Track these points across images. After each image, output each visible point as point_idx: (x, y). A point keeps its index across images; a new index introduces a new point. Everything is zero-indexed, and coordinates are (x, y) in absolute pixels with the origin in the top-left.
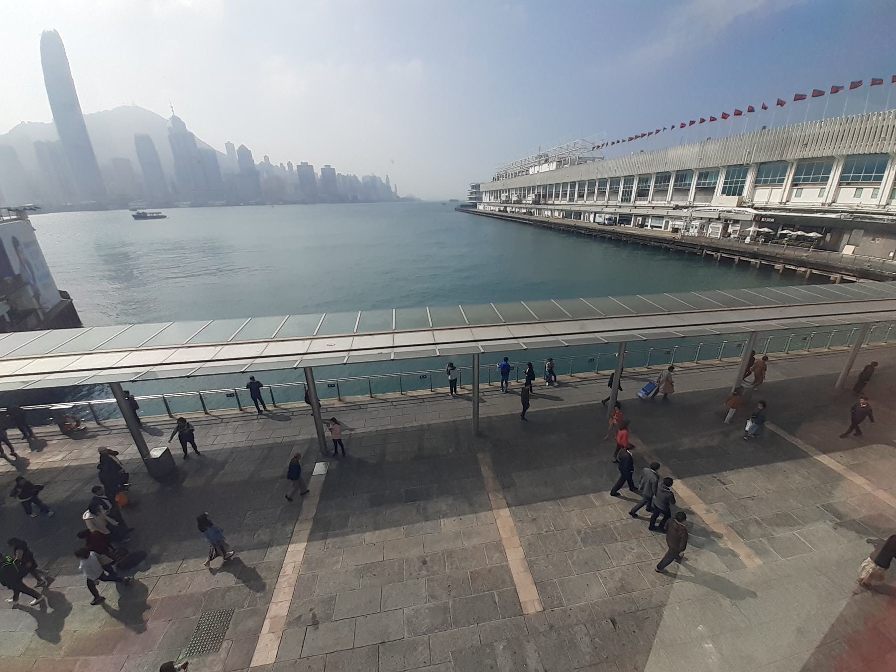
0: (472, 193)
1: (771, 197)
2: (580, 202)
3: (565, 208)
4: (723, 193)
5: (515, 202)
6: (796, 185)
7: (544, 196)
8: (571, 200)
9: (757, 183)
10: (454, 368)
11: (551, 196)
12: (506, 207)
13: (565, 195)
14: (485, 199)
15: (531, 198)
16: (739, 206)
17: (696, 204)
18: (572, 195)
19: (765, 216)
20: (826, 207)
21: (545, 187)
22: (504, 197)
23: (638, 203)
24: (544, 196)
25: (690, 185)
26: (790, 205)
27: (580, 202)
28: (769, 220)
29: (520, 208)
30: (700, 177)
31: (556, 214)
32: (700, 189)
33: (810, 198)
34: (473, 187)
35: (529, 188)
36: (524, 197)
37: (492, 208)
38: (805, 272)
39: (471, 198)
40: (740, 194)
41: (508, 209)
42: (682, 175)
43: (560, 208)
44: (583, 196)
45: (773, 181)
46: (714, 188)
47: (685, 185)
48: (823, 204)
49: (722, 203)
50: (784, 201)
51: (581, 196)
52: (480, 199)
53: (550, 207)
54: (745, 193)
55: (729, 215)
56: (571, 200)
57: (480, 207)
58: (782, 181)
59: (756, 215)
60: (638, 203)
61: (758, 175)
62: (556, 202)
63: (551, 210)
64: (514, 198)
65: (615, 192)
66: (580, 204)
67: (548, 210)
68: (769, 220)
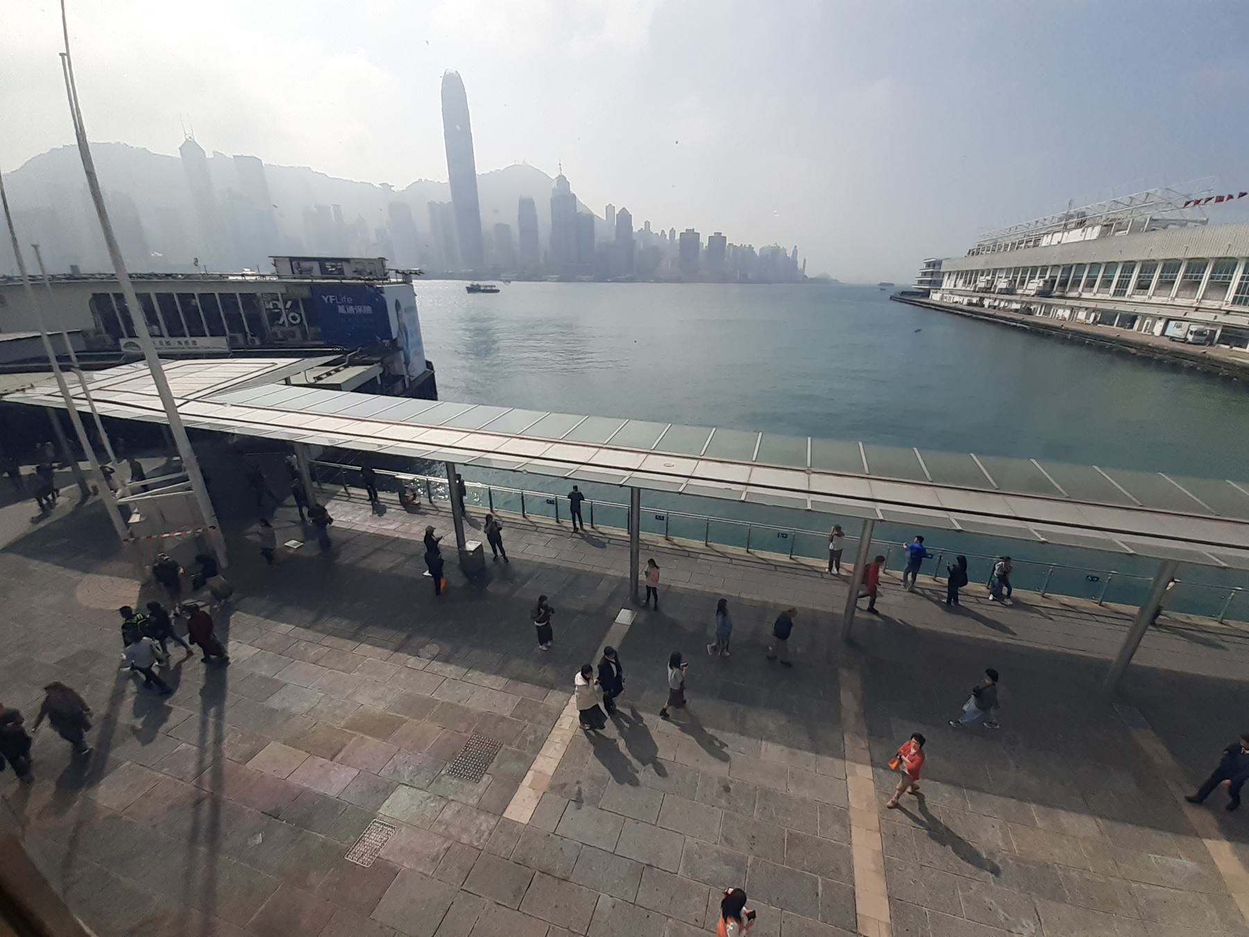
0: (925, 274)
2: (1137, 298)
3: (1101, 306)
5: (1001, 292)
7: (1063, 284)
8: (1121, 291)
10: (840, 534)
11: (1076, 283)
12: (982, 299)
14: (947, 284)
15: (1035, 285)
18: (1123, 285)
21: (1067, 269)
22: (982, 282)
24: (1063, 284)
27: (1137, 298)
31: (1082, 315)
34: (929, 265)
35: (1034, 270)
36: (1022, 283)
37: (957, 299)
41: (986, 302)
43: (1092, 305)
44: (1147, 287)
52: (937, 284)
53: (1069, 302)
56: (1121, 291)
57: (935, 297)
62: (1085, 295)
63: (1072, 309)
64: (1002, 284)
66: (1133, 301)
67: (1064, 307)
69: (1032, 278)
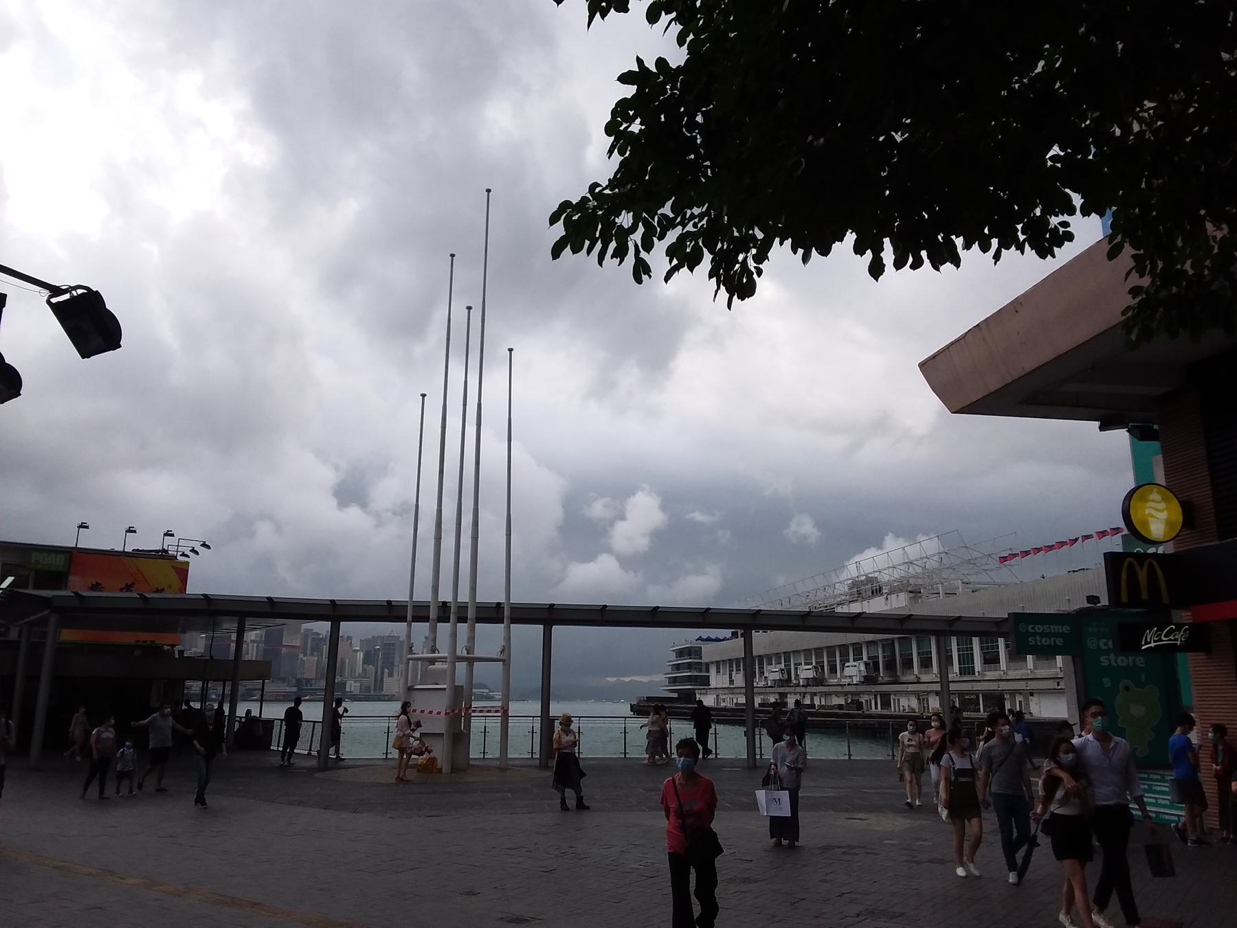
0: (678, 667)
2: (991, 675)
11: (908, 664)
12: (783, 695)
14: (717, 680)
24: (891, 665)
29: (827, 694)
34: (681, 653)
36: (833, 670)
41: (791, 701)
52: (705, 681)
53: (911, 688)
62: (924, 678)
63: (917, 694)
64: (806, 672)
66: (986, 678)
67: (907, 693)
69: (845, 660)
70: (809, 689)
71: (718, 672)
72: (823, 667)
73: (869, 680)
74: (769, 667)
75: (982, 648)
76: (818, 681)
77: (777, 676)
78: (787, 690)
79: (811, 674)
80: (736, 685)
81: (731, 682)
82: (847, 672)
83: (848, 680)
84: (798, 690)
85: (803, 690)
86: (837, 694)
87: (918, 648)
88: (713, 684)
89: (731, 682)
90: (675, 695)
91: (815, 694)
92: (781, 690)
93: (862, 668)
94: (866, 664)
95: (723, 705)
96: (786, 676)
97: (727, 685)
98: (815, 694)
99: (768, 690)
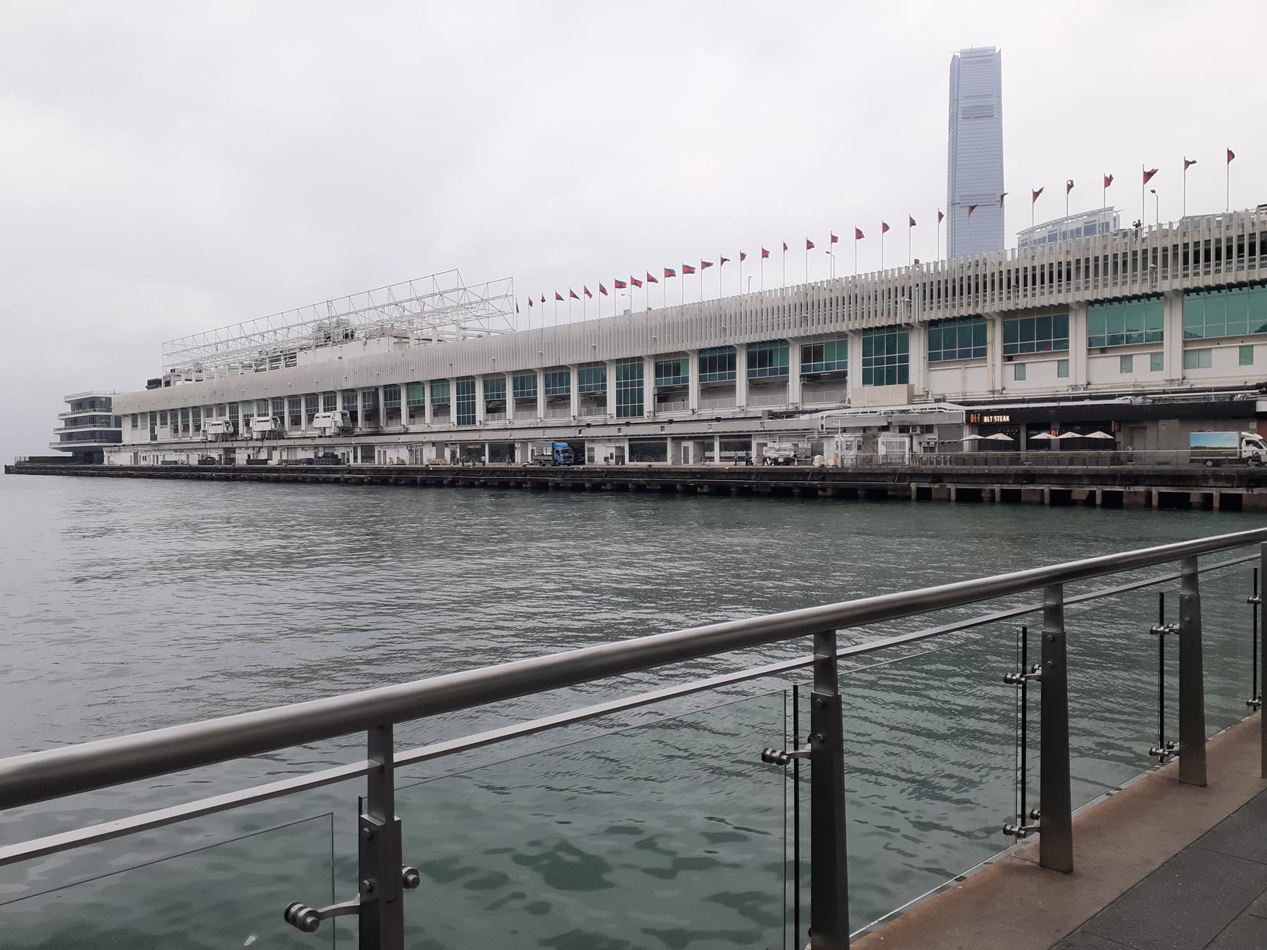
1: (986, 380)
4: (866, 380)
5: (265, 436)
6: (1010, 359)
7: (372, 415)
9: (933, 358)
11: (394, 413)
13: (441, 409)
15: (327, 421)
16: (911, 399)
17: (808, 407)
19: (988, 413)
20: (1081, 392)
22: (215, 425)
23: (664, 416)
24: (372, 415)
25: (785, 370)
26: (1011, 394)
28: (998, 419)
29: (289, 448)
30: (806, 357)
32: (811, 381)
33: (1041, 380)
36: (296, 421)
38: (1093, 494)
39: (70, 437)
40: (904, 379)
41: (241, 458)
42: (763, 354)
45: (965, 355)
46: (845, 374)
47: (773, 372)
48: (1075, 387)
49: (865, 399)
50: (998, 387)
51: (495, 408)
52: (117, 437)
54: (913, 378)
55: (908, 419)
57: (122, 459)
58: (981, 354)
59: (968, 412)
60: (664, 416)
61: (932, 344)
62: (413, 428)
64: (261, 424)
65: (594, 400)
66: (488, 428)
68: (998, 419)
70: (267, 443)
71: (135, 426)
72: (282, 419)
73: (345, 431)
74: (208, 420)
75: (486, 397)
76: (277, 435)
77: (220, 430)
78: (236, 444)
79: (268, 427)
80: (159, 440)
81: (154, 437)
82: (317, 423)
83: (317, 433)
84: (251, 444)
85: (259, 444)
86: (303, 447)
87: (408, 397)
88: (126, 439)
89: (154, 437)
90: (70, 454)
91: (275, 448)
92: (228, 445)
93: (338, 418)
94: (343, 415)
95: (143, 463)
96: (231, 429)
97: (149, 441)
98: (275, 448)
99: (208, 445)
